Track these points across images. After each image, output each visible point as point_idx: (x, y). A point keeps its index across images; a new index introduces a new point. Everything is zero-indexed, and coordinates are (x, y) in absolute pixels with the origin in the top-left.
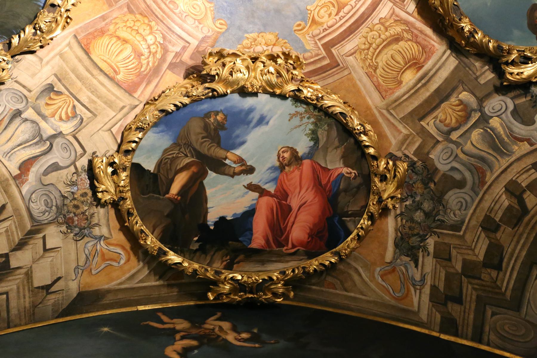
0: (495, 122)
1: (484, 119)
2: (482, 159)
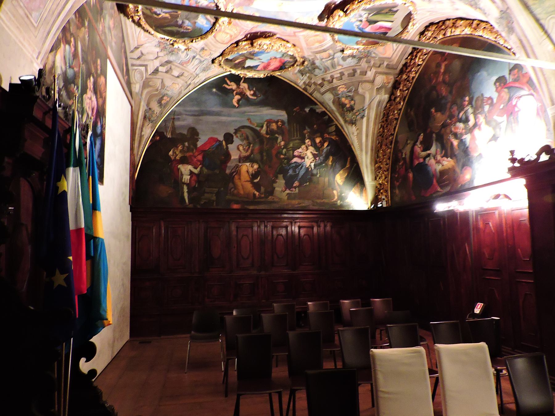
0: (336, 60)
1: (333, 58)
2: (328, 68)
